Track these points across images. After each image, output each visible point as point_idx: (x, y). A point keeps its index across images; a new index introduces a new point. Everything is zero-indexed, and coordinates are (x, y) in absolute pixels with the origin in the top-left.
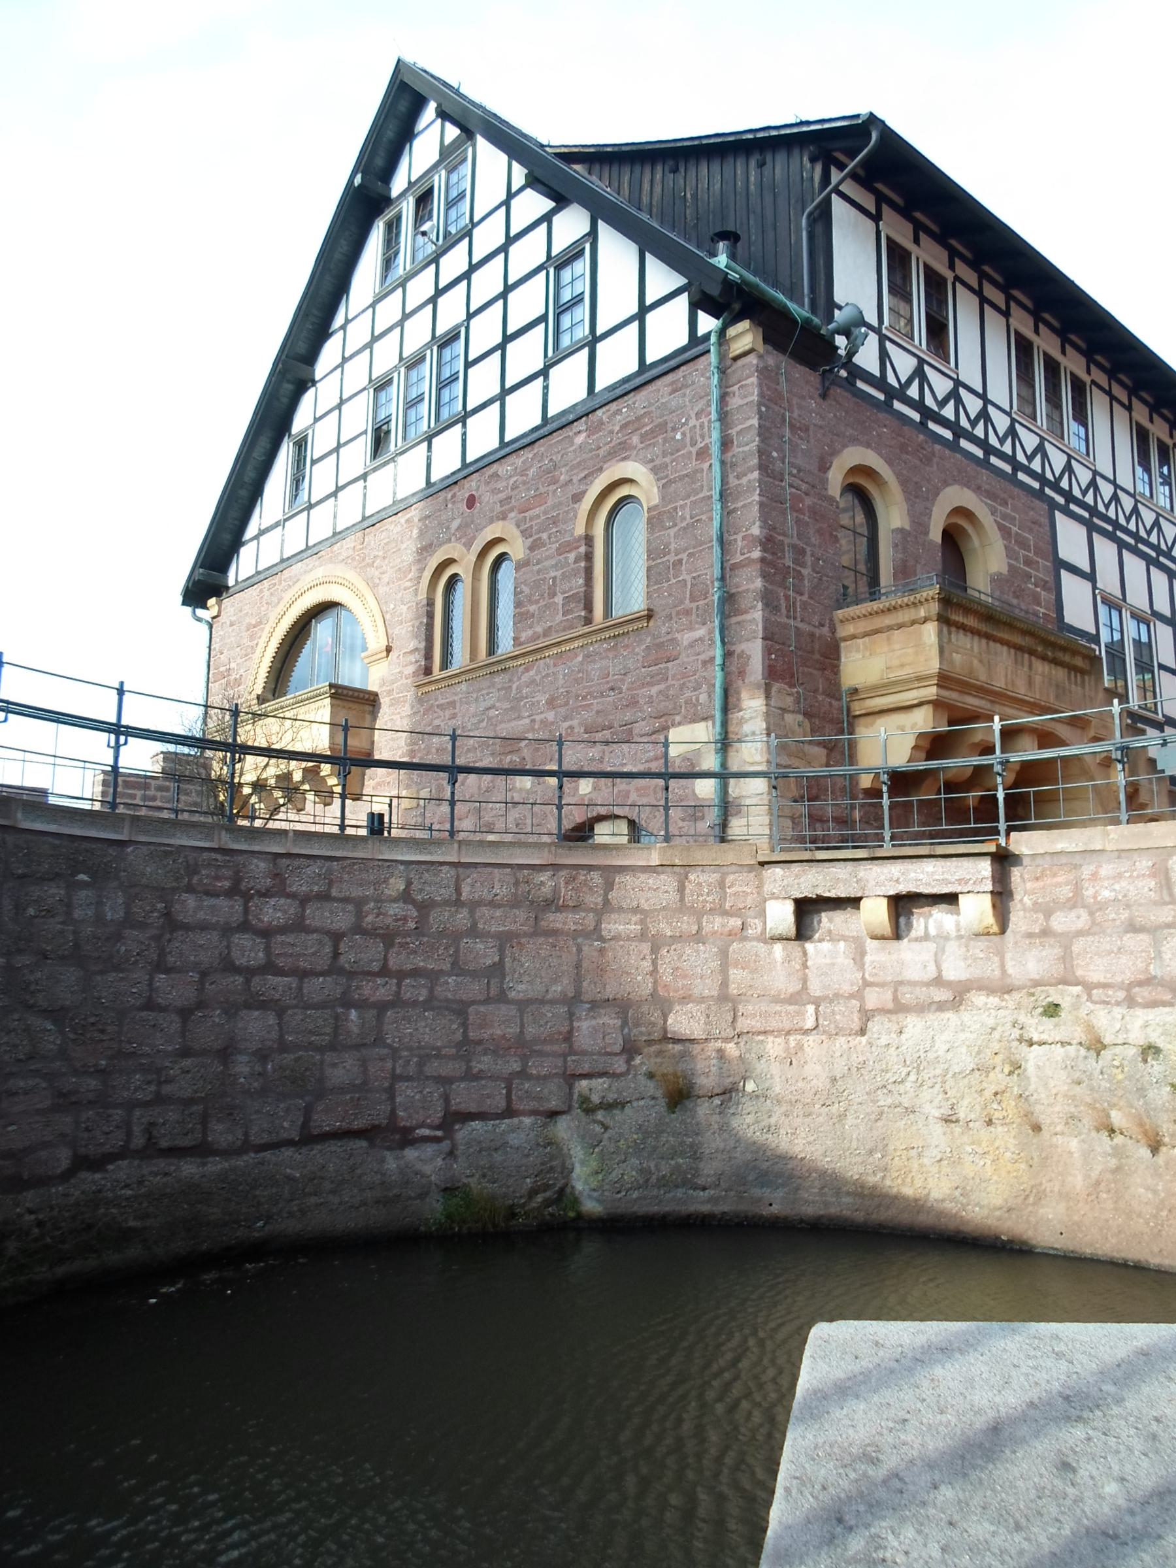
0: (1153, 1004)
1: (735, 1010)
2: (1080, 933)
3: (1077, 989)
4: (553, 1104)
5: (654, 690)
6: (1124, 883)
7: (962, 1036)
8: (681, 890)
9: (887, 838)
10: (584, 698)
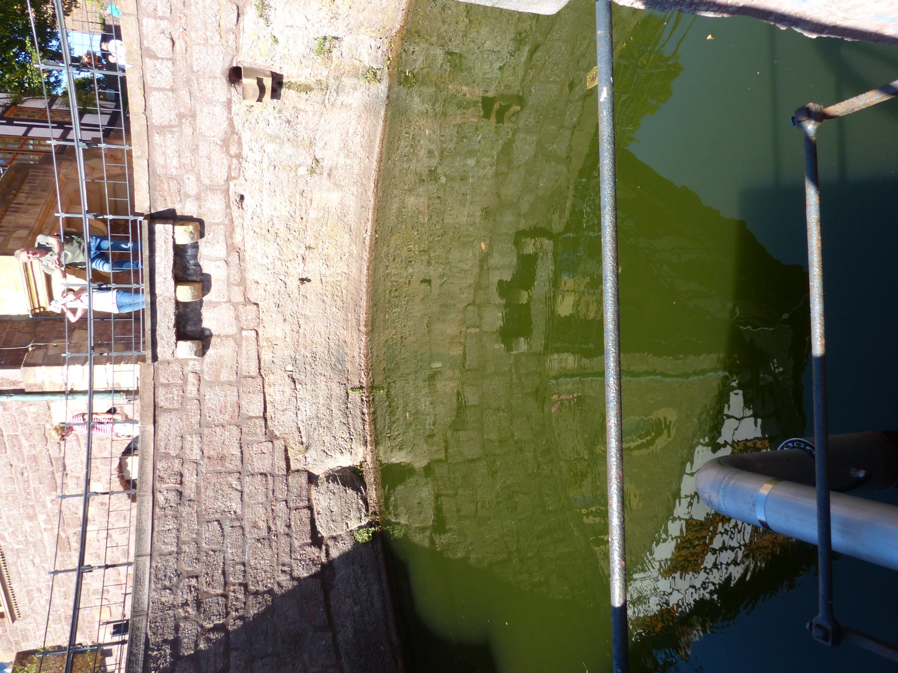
0: (240, 144)
2: (198, 179)
3: (232, 184)
4: (304, 479)
5: (25, 444)
6: (169, 152)
8: (169, 410)
9: (137, 286)
10: (29, 494)
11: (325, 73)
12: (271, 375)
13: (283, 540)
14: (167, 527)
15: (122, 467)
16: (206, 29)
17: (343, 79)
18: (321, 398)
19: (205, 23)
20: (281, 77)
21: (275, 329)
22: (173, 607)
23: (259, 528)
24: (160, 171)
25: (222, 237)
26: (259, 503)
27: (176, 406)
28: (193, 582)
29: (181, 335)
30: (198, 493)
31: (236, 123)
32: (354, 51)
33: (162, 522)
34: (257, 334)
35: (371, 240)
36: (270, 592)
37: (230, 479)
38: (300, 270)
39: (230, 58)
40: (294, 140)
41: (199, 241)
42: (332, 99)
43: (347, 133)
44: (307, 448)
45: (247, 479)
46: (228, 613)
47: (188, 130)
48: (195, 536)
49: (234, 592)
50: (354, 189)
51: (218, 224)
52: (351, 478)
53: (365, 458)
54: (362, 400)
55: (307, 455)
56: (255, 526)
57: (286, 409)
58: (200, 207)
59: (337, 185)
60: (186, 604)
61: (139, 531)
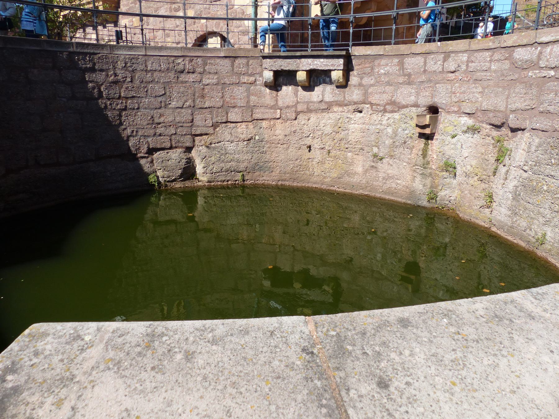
0: (392, 112)
1: (252, 111)
2: (372, 85)
3: (368, 106)
4: (188, 144)
7: (329, 121)
8: (233, 66)
9: (309, 47)
11: (434, 167)
12: (253, 127)
13: (152, 132)
14: (162, 64)
15: (213, 34)
16: (461, 93)
17: (430, 178)
18: (238, 156)
19: (464, 93)
20: (432, 139)
21: (280, 129)
22: (114, 68)
23: (159, 118)
24: (377, 62)
25: (336, 99)
26: (175, 118)
27: (235, 70)
28: (129, 79)
29: (277, 74)
30: (182, 82)
31: (405, 110)
32: (447, 186)
33: (166, 61)
34: (278, 119)
35: (333, 190)
36: (121, 124)
37: (190, 101)
38: (316, 146)
39: (444, 107)
40: (393, 146)
41: (334, 85)
42: (418, 171)
43: (398, 179)
44: (207, 147)
45: (190, 111)
46: (109, 99)
47: (401, 80)
48: (156, 80)
49: (122, 103)
50: (364, 181)
51: (344, 97)
52: (189, 172)
53: (201, 181)
54: (236, 181)
55: (203, 147)
56: (161, 115)
57: (232, 135)
58: (355, 86)
59: (366, 171)
60: (116, 75)
61: (161, 48)
